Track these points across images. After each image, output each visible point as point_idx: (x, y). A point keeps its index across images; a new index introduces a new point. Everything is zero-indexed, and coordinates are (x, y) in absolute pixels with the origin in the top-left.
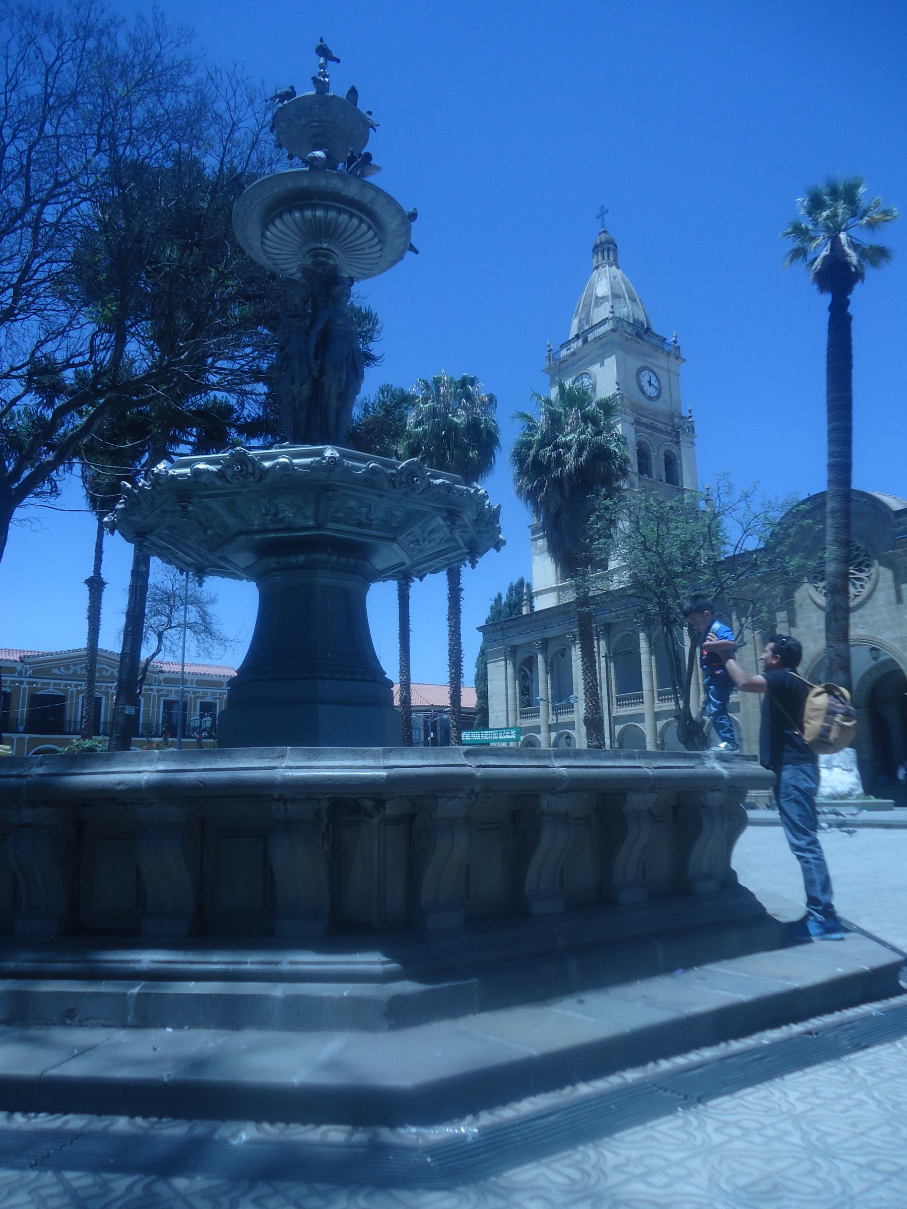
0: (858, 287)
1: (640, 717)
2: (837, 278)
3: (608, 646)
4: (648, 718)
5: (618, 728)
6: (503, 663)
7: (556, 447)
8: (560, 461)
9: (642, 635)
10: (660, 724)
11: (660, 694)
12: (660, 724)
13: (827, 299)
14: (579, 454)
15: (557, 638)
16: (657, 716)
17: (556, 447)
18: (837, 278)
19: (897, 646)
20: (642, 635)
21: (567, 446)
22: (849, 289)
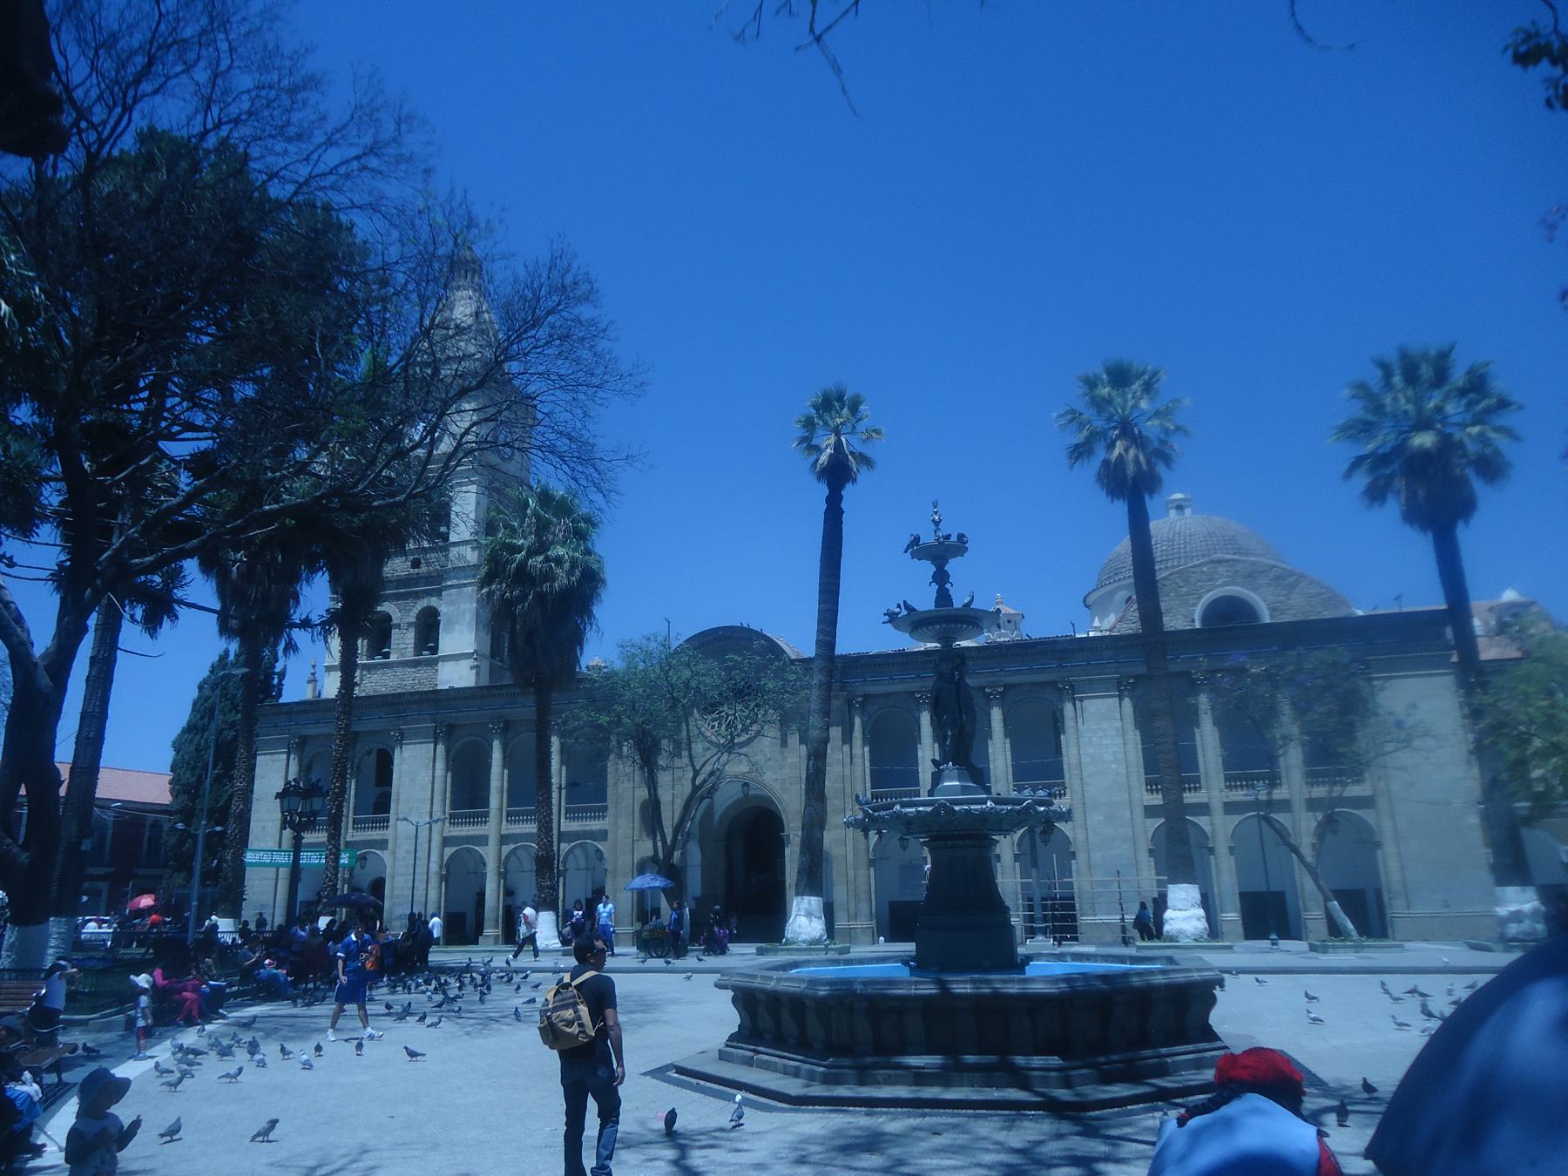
0: (849, 486)
1: (483, 840)
2: (837, 474)
3: (448, 750)
4: (493, 841)
5: (449, 851)
6: (284, 756)
7: (547, 559)
8: (548, 576)
9: (496, 745)
10: (506, 849)
11: (509, 814)
12: (506, 849)
13: (824, 490)
14: (570, 573)
15: (374, 733)
16: (504, 839)
17: (547, 559)
18: (837, 474)
19: (776, 786)
20: (496, 745)
21: (559, 561)
22: (842, 486)
